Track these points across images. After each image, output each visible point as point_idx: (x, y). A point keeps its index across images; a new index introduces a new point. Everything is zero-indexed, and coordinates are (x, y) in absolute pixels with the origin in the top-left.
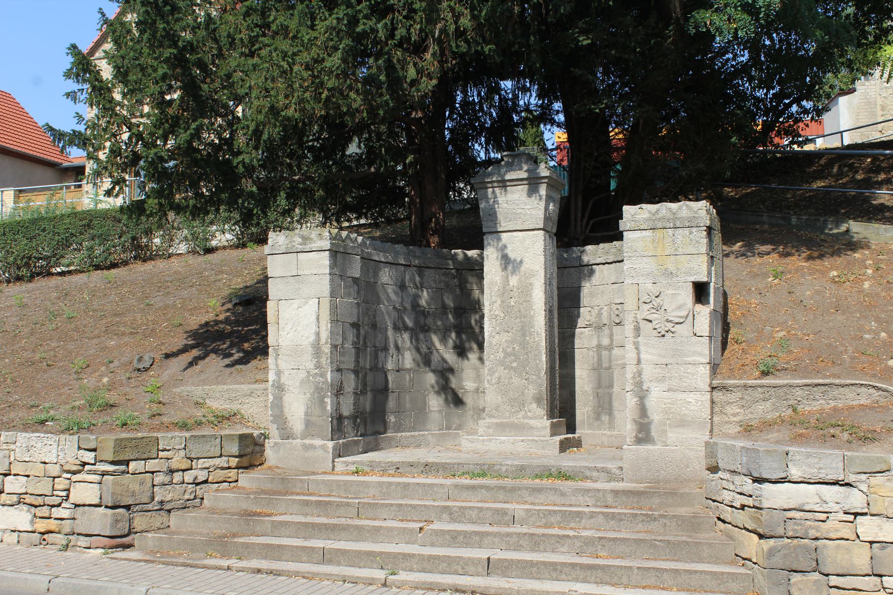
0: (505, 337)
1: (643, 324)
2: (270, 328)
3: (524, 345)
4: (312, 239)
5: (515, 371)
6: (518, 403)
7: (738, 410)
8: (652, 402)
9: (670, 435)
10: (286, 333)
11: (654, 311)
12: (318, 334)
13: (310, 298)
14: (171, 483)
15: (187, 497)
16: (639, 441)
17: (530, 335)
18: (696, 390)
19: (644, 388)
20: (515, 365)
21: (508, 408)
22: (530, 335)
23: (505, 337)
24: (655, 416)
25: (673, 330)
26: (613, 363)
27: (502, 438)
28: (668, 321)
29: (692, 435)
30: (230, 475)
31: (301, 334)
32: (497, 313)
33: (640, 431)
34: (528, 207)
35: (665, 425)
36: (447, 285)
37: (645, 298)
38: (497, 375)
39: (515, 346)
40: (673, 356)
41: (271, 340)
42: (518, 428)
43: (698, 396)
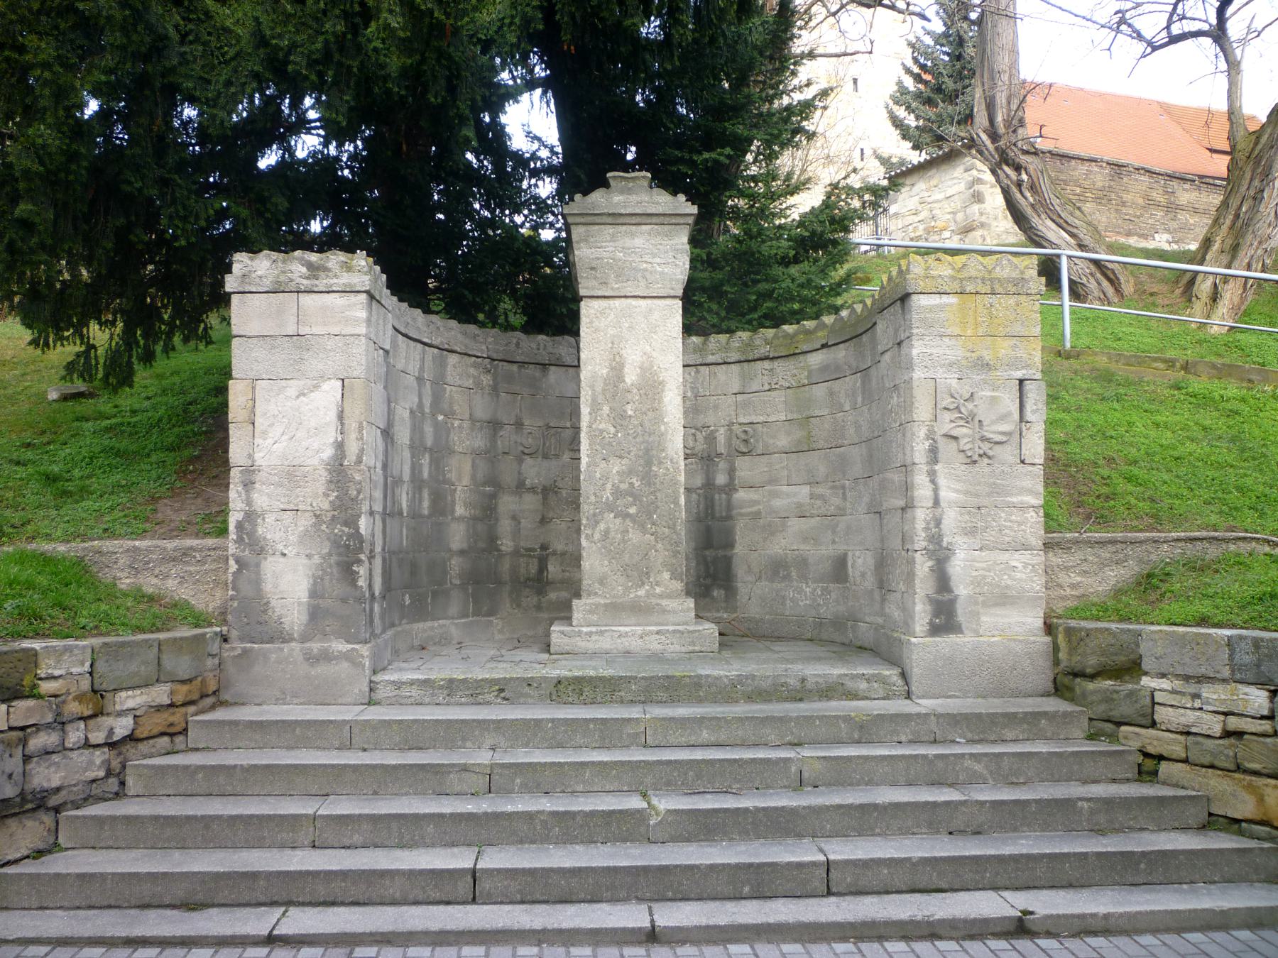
0: (616, 467)
1: (942, 443)
2: (233, 431)
3: (648, 478)
4: (329, 270)
5: (634, 521)
6: (641, 573)
7: (1079, 579)
8: (957, 567)
9: (984, 619)
10: (270, 441)
11: (962, 423)
12: (340, 446)
13: (323, 378)
14: (63, 748)
15: (91, 775)
16: (935, 630)
17: (660, 463)
18: (1026, 547)
19: (945, 544)
20: (632, 510)
21: (622, 580)
22: (660, 463)
23: (616, 467)
24: (962, 590)
25: (990, 453)
26: (734, 512)
27: (621, 628)
28: (983, 439)
29: (1019, 619)
30: (171, 719)
31: (305, 444)
32: (602, 426)
33: (937, 614)
34: (658, 260)
35: (976, 603)
36: (478, 384)
37: (947, 402)
38: (602, 526)
39: (634, 480)
40: (989, 495)
41: (237, 452)
42: (639, 610)
43: (1025, 556)
